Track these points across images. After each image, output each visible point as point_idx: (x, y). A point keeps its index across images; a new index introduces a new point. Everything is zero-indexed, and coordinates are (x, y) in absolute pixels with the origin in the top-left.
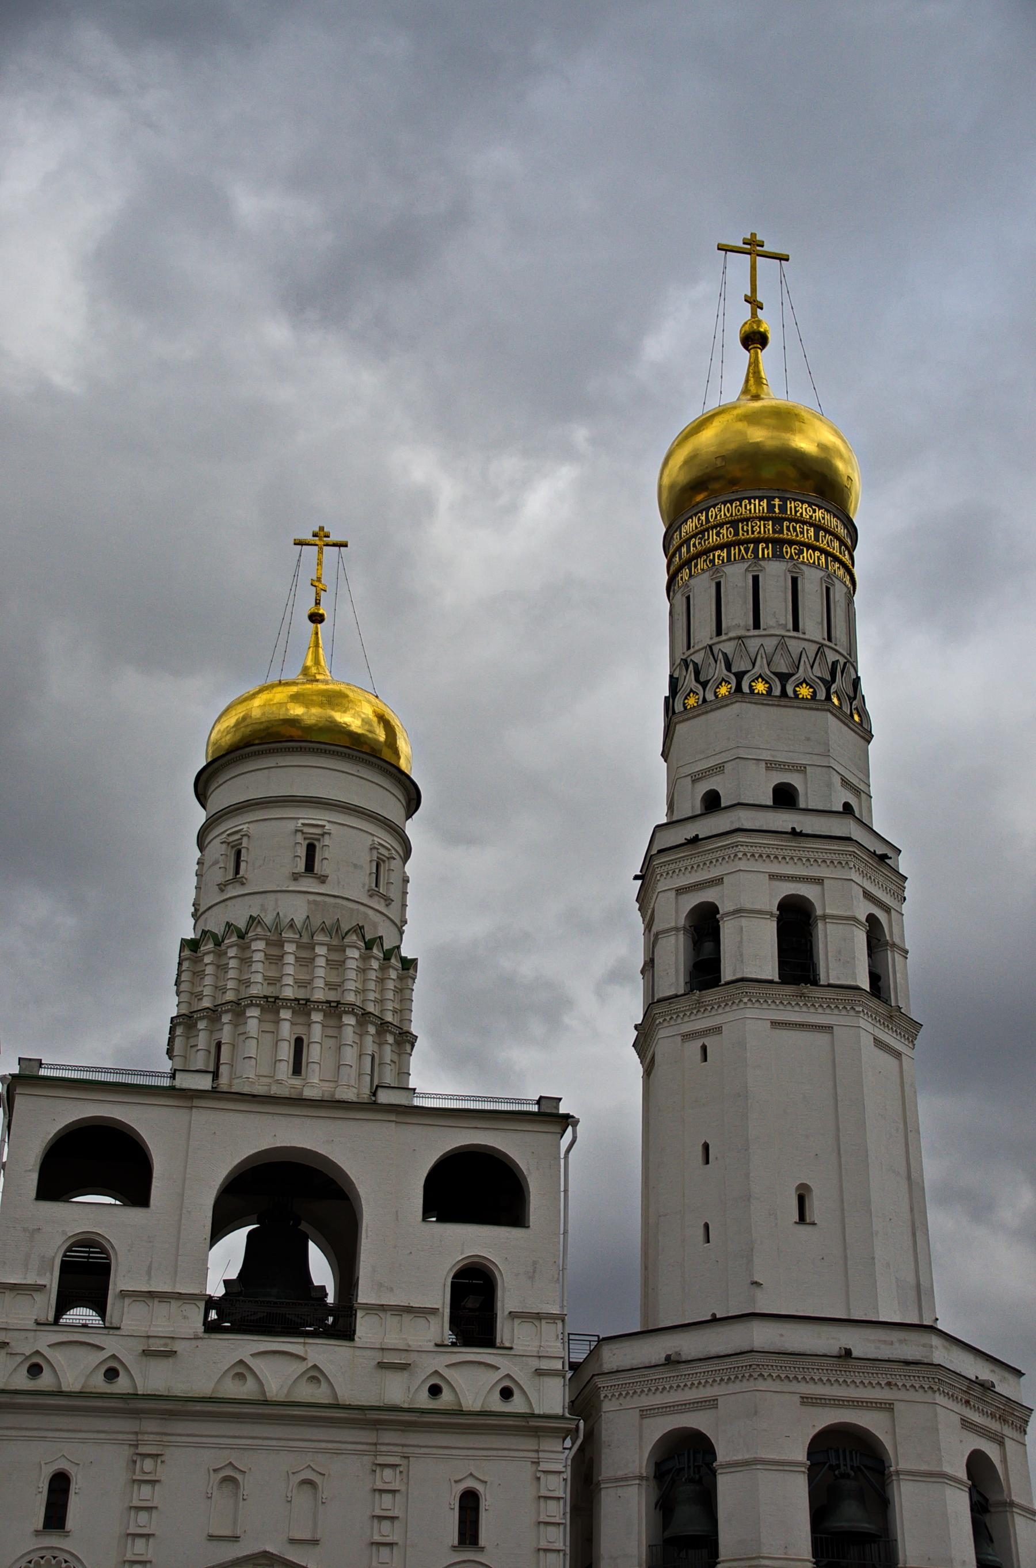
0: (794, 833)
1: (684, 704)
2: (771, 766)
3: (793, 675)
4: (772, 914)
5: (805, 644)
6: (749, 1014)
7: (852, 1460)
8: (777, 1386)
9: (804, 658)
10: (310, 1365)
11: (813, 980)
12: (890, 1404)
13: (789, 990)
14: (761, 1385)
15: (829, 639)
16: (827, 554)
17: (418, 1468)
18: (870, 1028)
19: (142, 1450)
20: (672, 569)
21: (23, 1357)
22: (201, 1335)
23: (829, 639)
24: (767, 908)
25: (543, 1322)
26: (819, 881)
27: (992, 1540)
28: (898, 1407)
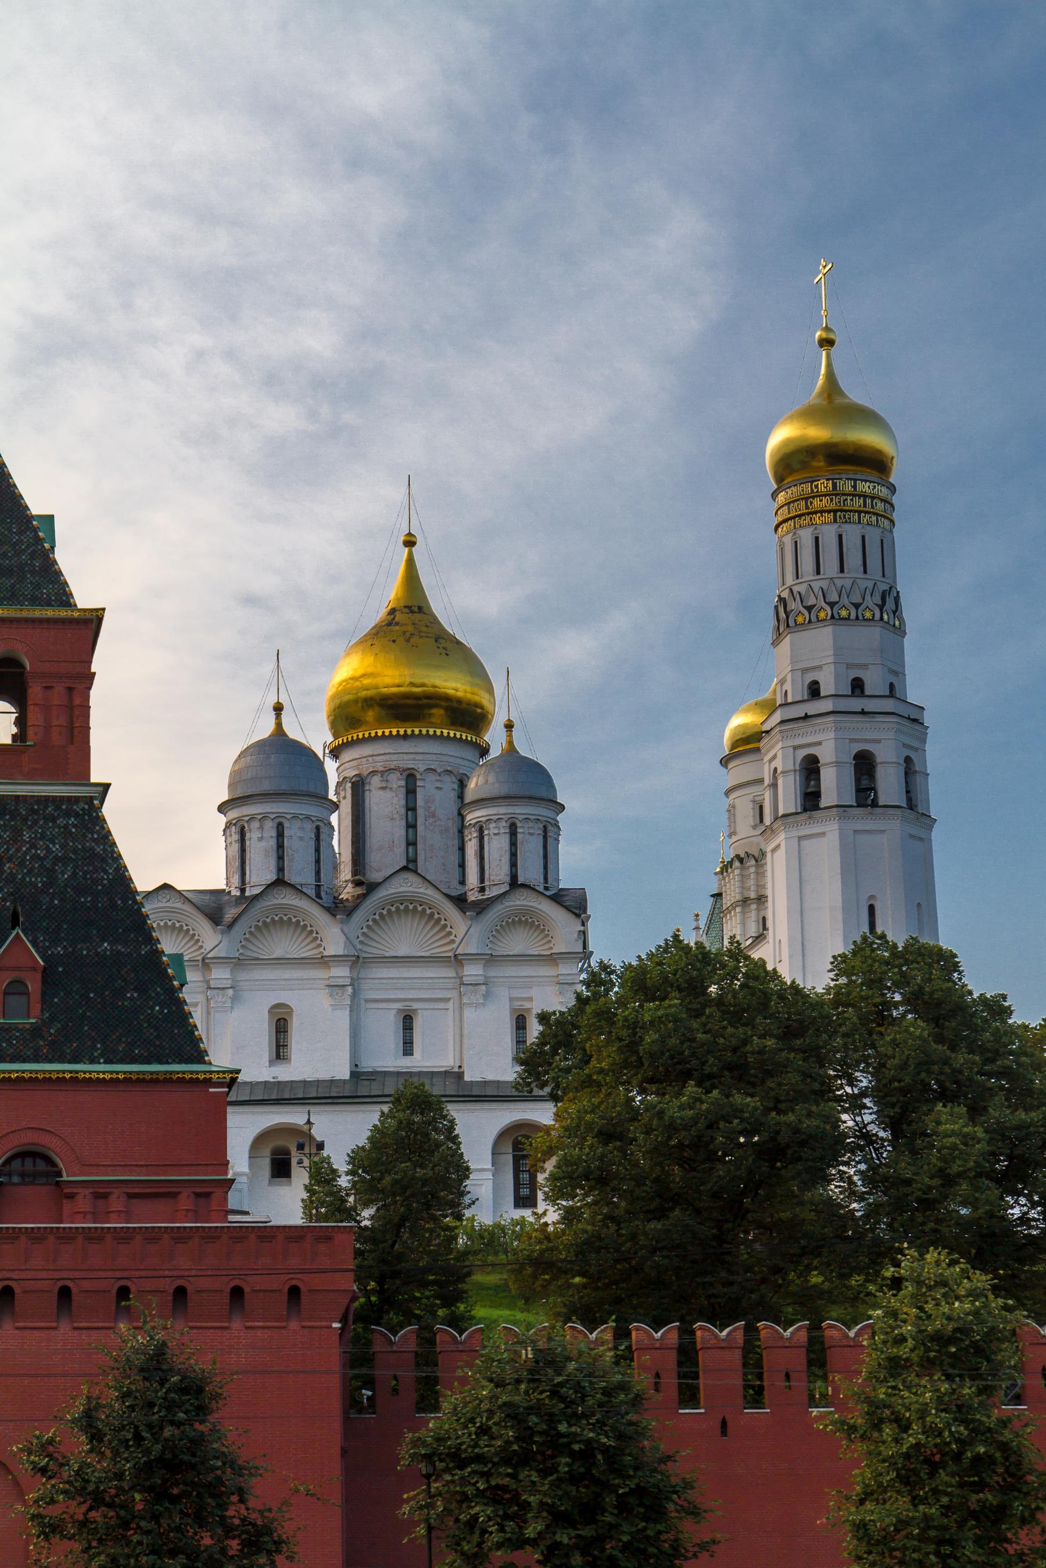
0: (863, 713)
1: (795, 620)
2: (849, 666)
4: (851, 763)
9: (868, 591)
26: (878, 741)
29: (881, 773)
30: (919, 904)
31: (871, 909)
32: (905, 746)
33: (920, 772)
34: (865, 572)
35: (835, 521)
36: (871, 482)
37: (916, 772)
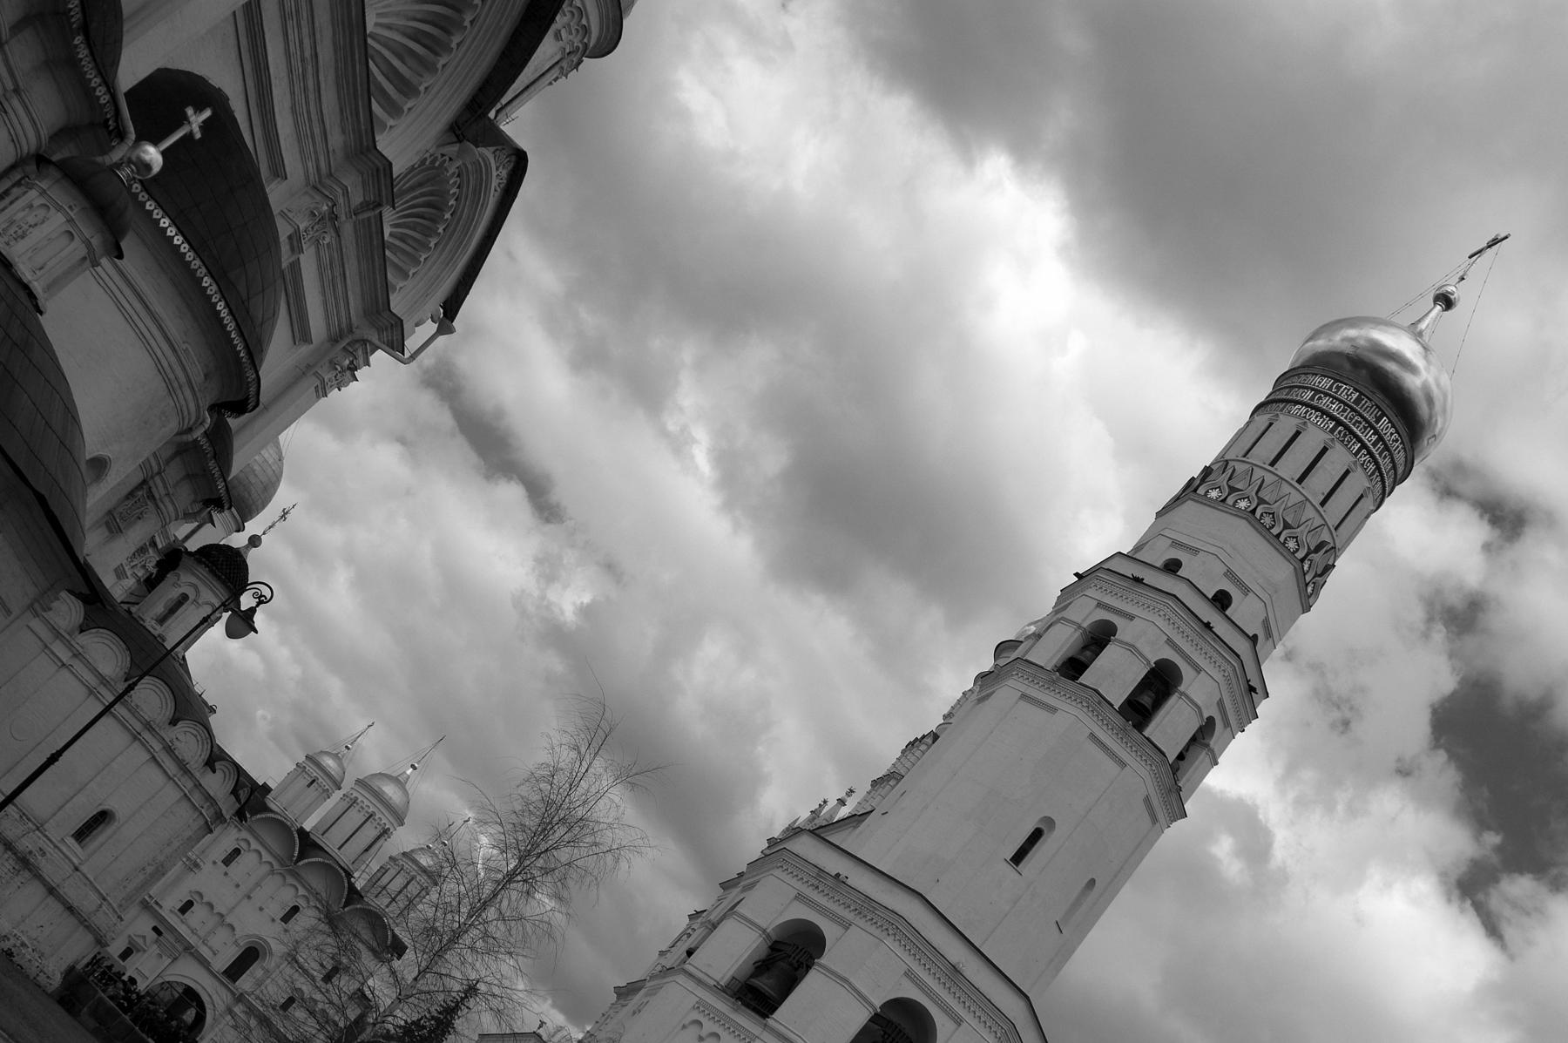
0: (1208, 626)
2: (1230, 575)
3: (1291, 528)
4: (1149, 662)
5: (1317, 516)
9: (1309, 522)
11: (1140, 726)
13: (1118, 720)
16: (1378, 468)
20: (1271, 398)
26: (1198, 669)
28: (965, 1024)
29: (1173, 706)
30: (1092, 883)
31: (1036, 835)
32: (1220, 703)
33: (1212, 751)
34: (1323, 504)
35: (1332, 431)
36: (1397, 432)
37: (1207, 746)
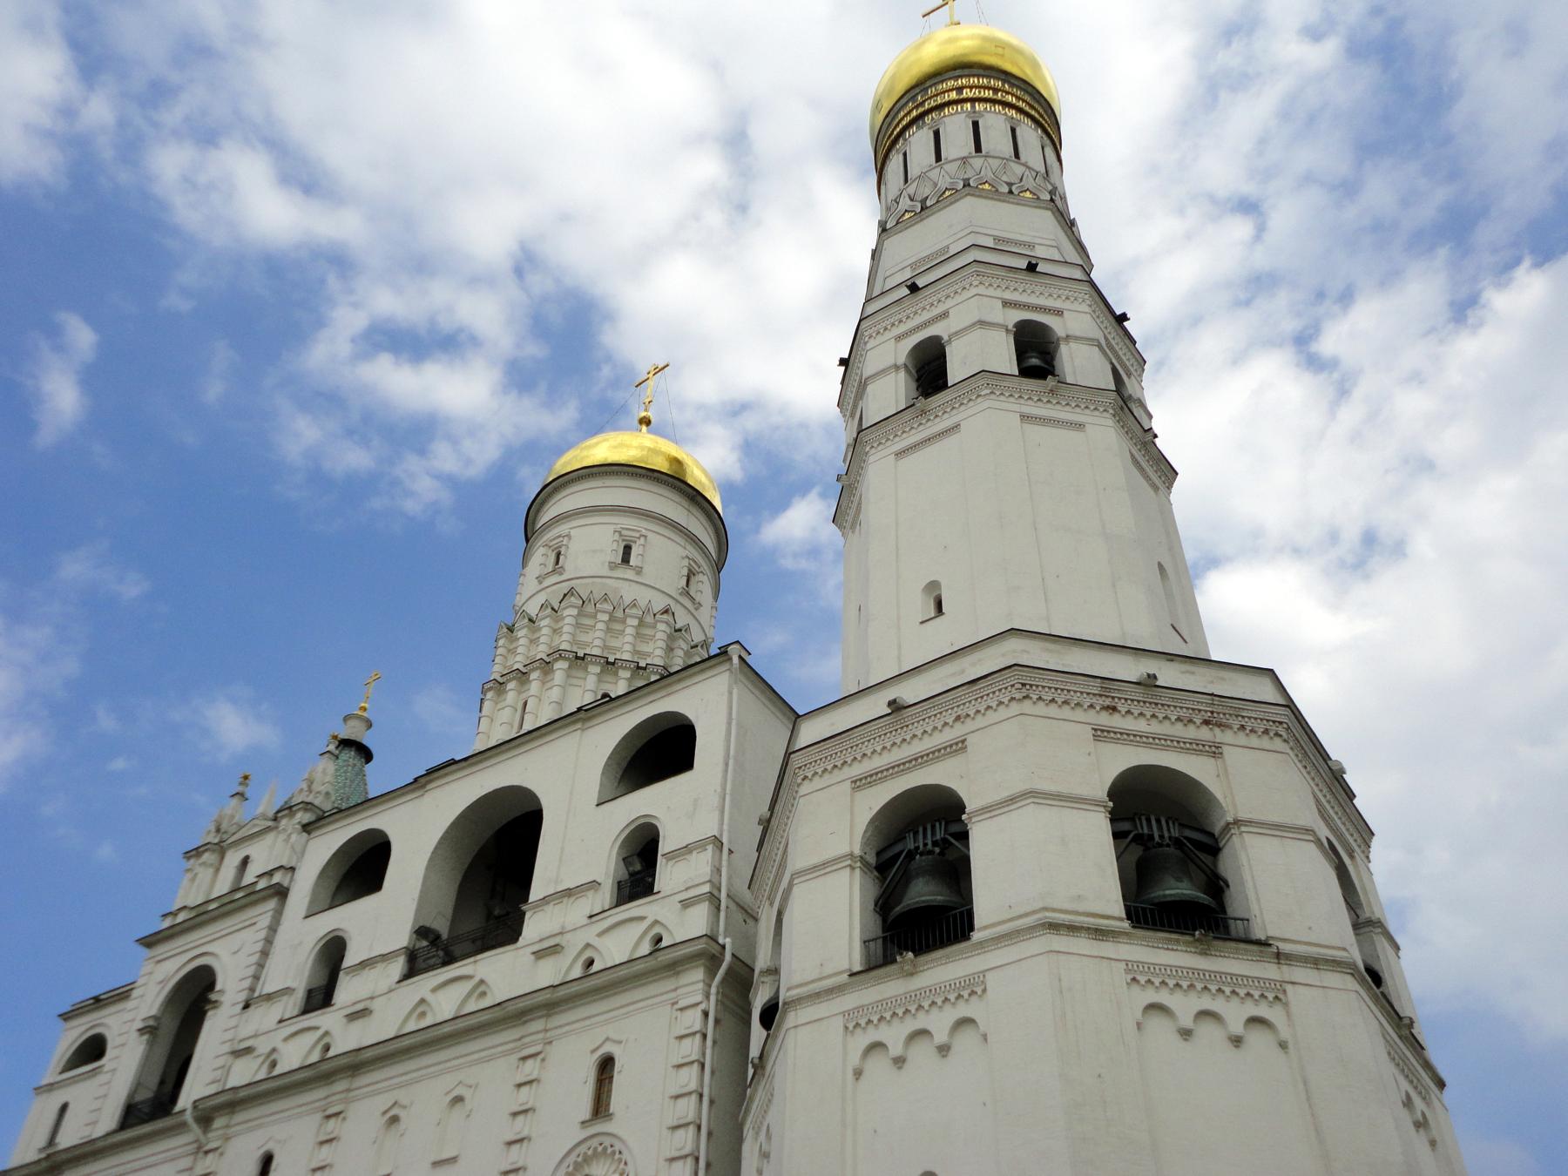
4: (897, 367)
6: (872, 459)
7: (933, 834)
8: (827, 779)
10: (477, 980)
12: (963, 741)
14: (806, 788)
15: (978, 148)
17: (557, 1052)
18: (1016, 407)
19: (331, 1111)
21: (261, 1059)
22: (393, 987)
23: (978, 148)
24: (891, 361)
25: (695, 853)
26: (945, 315)
27: (1228, 886)
28: (970, 740)
32: (1006, 304)
